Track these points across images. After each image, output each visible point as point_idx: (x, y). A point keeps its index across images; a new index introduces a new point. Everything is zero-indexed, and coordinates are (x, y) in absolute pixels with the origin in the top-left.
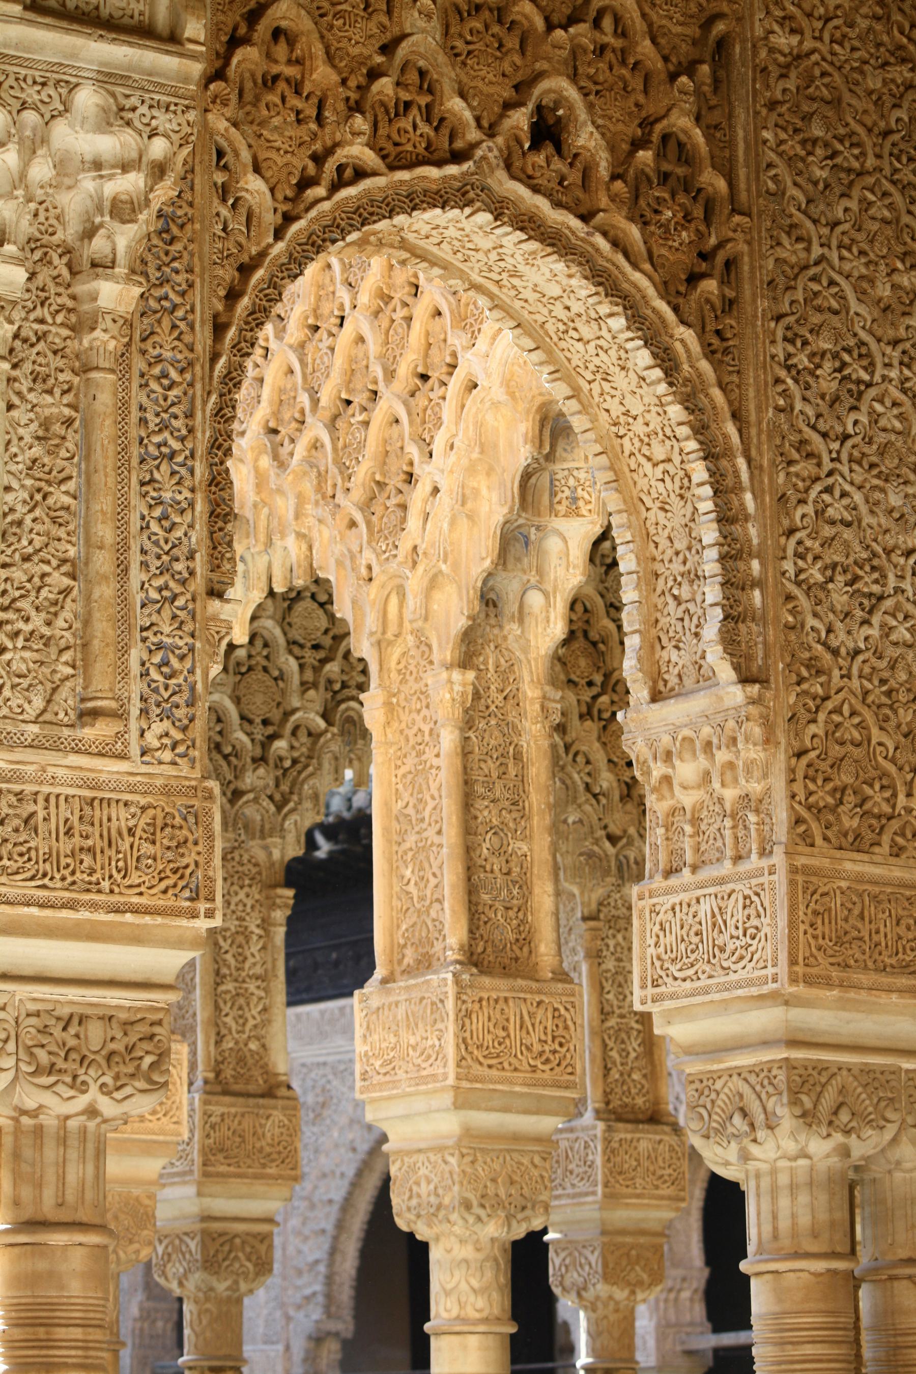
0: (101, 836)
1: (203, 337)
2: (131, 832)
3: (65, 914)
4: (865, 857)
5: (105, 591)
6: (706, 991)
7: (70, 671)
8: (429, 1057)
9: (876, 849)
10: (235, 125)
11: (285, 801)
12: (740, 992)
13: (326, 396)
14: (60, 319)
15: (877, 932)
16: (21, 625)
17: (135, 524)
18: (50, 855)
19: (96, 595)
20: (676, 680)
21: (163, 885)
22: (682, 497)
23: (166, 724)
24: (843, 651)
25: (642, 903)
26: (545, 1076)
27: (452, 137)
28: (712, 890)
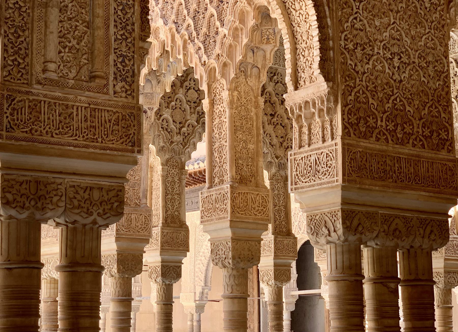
0: (98, 122)
2: (110, 121)
3: (84, 150)
4: (367, 141)
5: (100, 33)
6: (313, 186)
7: (86, 62)
8: (222, 211)
9: (371, 139)
11: (186, 145)
12: (325, 186)
13: (192, 11)
15: (372, 166)
16: (67, 44)
17: (112, 11)
18: (79, 128)
19: (96, 34)
20: (303, 83)
22: (305, 21)
23: (123, 83)
24: (360, 72)
25: (291, 158)
26: (259, 217)
28: (315, 152)
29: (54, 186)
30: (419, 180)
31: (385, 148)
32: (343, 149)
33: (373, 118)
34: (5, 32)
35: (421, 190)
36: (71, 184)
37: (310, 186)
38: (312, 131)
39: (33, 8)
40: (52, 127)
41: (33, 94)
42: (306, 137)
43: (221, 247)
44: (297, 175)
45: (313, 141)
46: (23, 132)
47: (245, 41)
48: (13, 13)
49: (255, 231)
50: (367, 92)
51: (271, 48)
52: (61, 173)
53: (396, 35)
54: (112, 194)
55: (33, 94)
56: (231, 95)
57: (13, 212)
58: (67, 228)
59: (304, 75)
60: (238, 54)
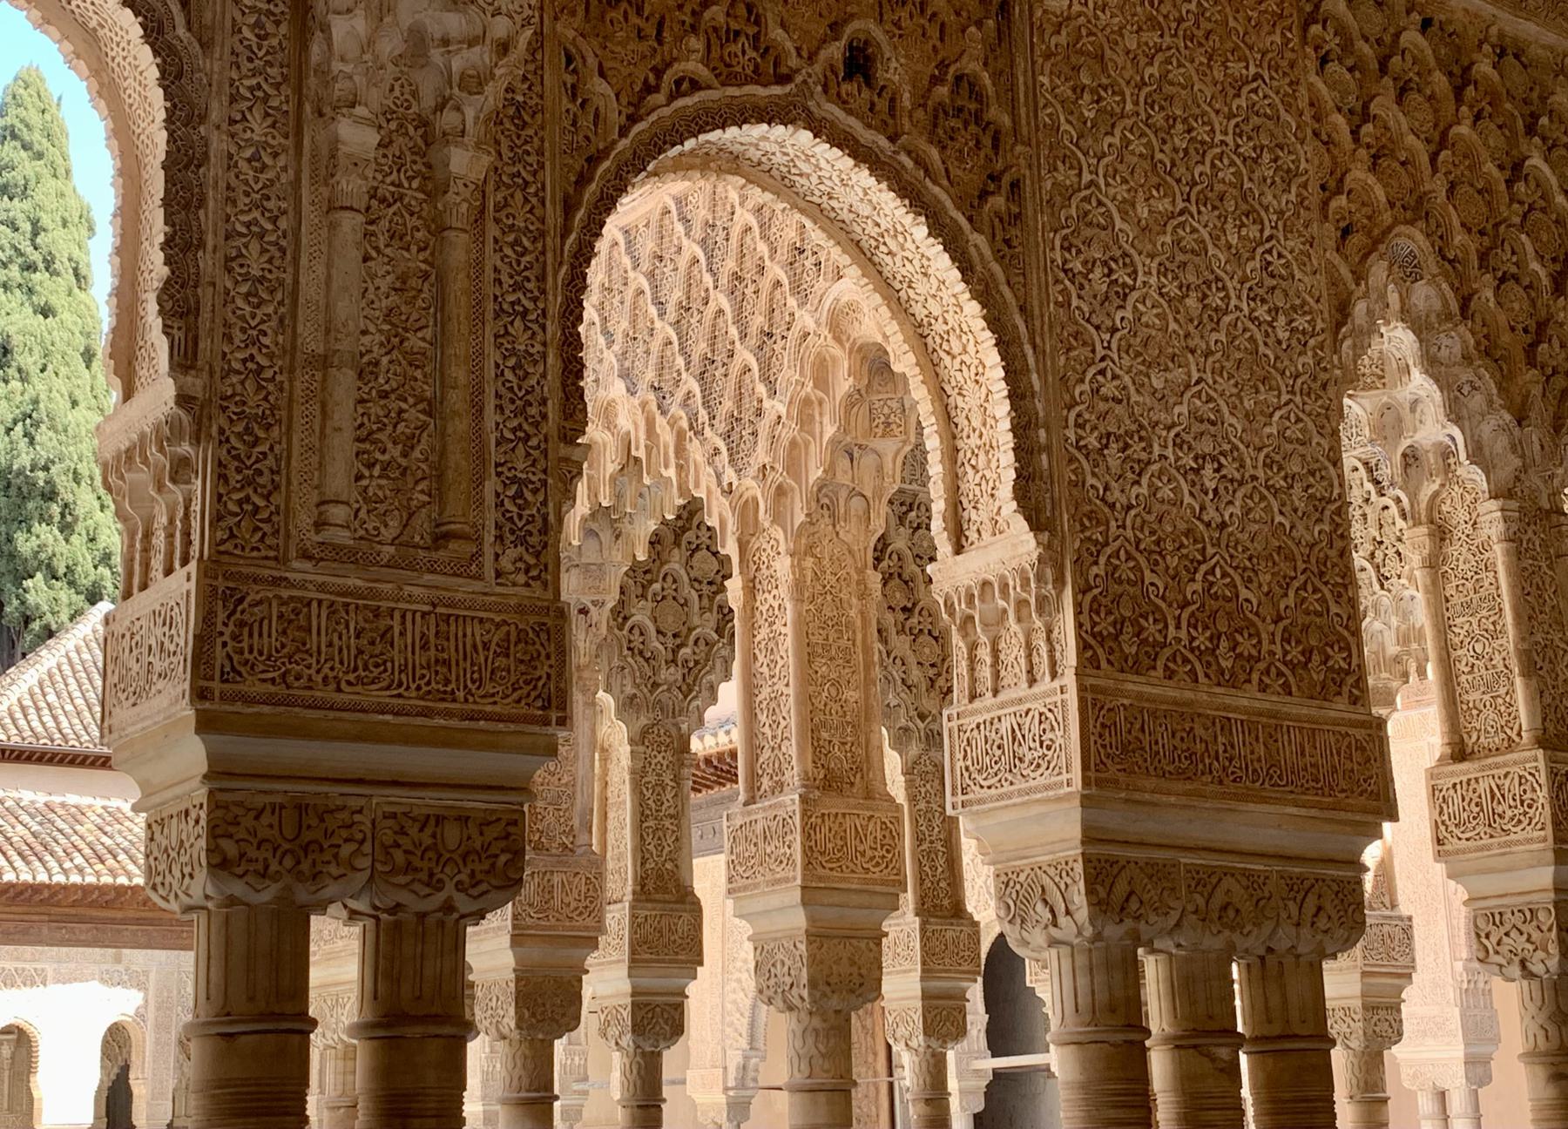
0: (457, 650)
1: (553, 215)
2: (486, 646)
3: (419, 721)
5: (459, 426)
6: (1009, 796)
9: (1152, 673)
10: (582, 35)
11: (690, 691)
12: (1039, 796)
13: (695, 358)
14: (415, 184)
15: (1157, 743)
16: (378, 455)
17: (490, 372)
19: (450, 431)
21: (516, 695)
23: (520, 549)
24: (1118, 505)
27: (776, 65)
28: (1012, 710)
29: (343, 816)
30: (1280, 777)
31: (1189, 695)
32: (1082, 701)
33: (1155, 621)
34: (222, 431)
35: (1285, 802)
36: (387, 809)
37: (1000, 797)
38: (1002, 657)
39: (292, 371)
40: (337, 665)
41: (291, 585)
42: (985, 672)
43: (780, 956)
44: (967, 769)
45: (1005, 682)
46: (264, 681)
47: (830, 430)
48: (242, 383)
49: (866, 912)
50: (1137, 555)
51: (895, 448)
52: (360, 782)
53: (1206, 410)
54: (492, 832)
55: (291, 585)
56: (798, 568)
57: (238, 888)
58: (378, 925)
59: (977, 517)
60: (812, 465)
